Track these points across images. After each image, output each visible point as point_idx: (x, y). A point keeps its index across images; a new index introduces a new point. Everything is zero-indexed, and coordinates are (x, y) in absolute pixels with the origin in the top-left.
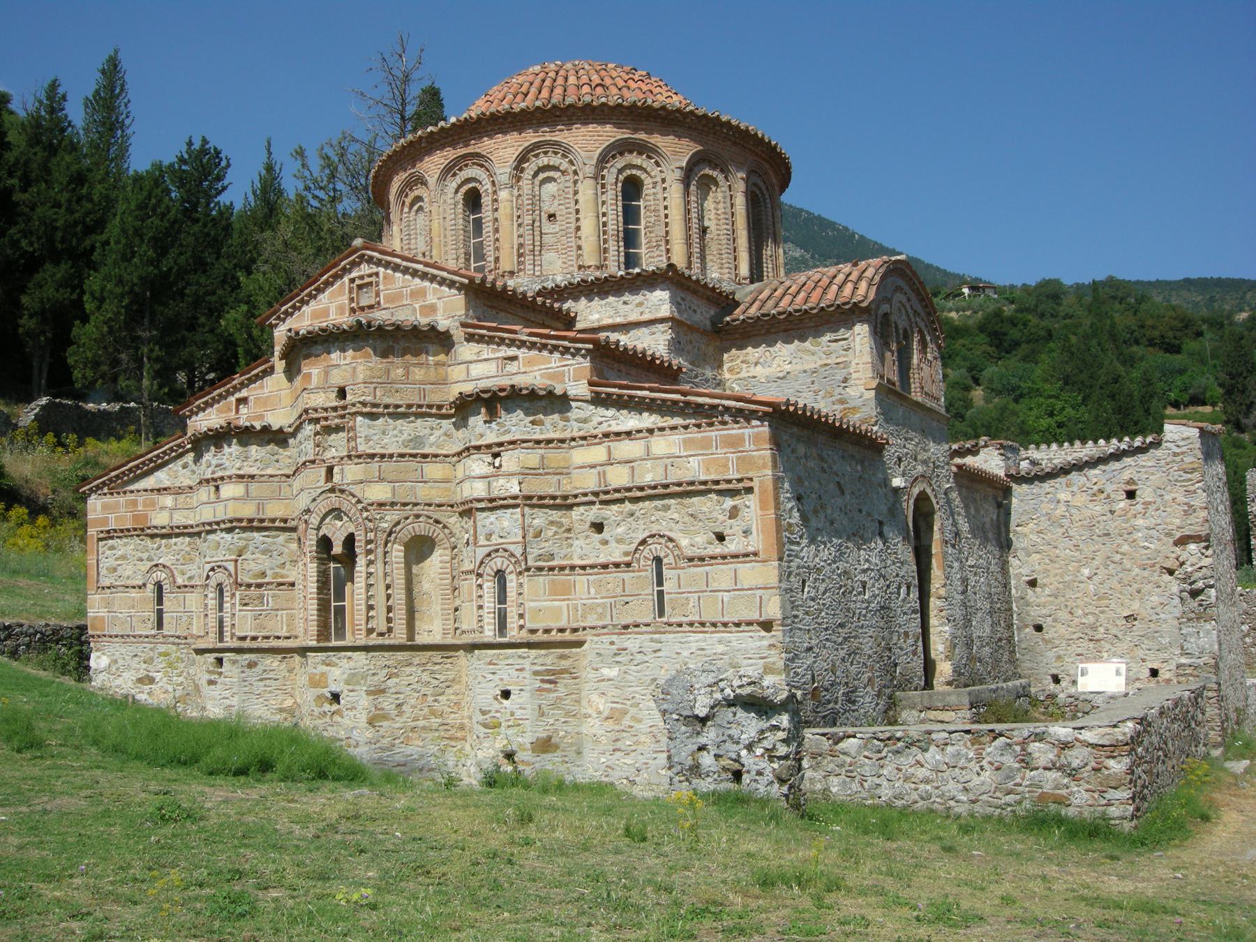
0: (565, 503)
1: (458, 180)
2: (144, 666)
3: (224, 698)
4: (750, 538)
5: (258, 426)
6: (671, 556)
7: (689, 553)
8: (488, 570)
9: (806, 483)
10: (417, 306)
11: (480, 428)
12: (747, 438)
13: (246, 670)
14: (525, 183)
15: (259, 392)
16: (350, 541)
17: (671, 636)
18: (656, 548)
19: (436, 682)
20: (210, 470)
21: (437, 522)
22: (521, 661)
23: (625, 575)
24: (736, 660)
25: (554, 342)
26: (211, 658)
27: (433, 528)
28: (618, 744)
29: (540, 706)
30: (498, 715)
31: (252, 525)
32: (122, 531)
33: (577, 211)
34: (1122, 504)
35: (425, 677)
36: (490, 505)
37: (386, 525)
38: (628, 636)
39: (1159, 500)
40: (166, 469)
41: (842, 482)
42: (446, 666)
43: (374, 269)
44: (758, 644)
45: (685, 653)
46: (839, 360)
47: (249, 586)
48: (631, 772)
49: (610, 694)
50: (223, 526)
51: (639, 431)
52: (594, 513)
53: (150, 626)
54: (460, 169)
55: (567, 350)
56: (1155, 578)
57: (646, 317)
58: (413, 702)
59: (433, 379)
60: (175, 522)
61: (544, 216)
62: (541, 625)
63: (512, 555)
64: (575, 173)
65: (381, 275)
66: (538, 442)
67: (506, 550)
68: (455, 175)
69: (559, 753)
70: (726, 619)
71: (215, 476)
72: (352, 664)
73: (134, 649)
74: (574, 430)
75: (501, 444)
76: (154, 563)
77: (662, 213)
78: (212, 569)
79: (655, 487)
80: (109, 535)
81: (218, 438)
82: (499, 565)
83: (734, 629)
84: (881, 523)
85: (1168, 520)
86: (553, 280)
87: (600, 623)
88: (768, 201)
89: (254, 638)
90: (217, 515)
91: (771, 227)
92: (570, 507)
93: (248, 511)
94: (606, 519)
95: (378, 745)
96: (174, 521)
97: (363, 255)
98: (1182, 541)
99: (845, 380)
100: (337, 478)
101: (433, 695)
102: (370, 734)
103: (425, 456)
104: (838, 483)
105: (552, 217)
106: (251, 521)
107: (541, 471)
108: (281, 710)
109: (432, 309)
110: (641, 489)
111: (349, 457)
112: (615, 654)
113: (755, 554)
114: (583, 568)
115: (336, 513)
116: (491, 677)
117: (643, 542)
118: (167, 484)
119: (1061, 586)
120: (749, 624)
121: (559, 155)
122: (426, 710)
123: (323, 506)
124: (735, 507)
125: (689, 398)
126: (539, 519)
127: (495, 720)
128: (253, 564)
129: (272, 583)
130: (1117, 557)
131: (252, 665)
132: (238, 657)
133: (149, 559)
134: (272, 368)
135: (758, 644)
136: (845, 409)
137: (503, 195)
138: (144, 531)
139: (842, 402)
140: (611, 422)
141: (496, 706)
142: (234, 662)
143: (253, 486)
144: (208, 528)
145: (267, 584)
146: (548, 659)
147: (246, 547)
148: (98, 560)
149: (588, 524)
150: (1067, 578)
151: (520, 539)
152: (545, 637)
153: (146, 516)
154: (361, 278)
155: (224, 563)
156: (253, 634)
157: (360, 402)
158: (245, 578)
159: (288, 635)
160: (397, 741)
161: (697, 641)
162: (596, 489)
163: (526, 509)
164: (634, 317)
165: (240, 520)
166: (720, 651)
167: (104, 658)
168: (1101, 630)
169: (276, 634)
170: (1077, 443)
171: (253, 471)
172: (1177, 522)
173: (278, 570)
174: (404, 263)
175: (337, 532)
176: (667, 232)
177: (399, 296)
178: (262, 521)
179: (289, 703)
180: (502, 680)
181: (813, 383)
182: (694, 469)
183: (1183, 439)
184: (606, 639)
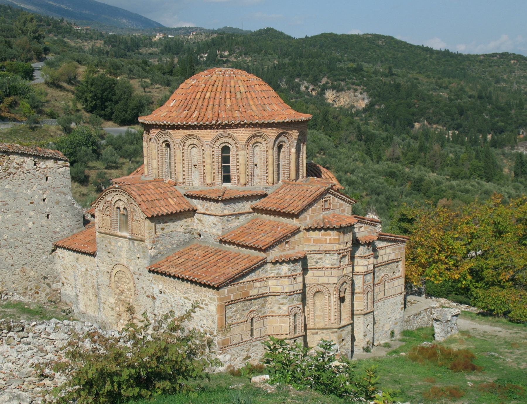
20: (290, 272)
32: (235, 300)
60: (260, 292)
71: (293, 274)
73: (242, 347)
153: (248, 292)
167: (228, 355)
182: (392, 257)
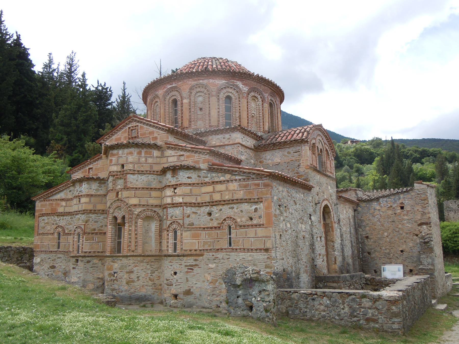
0: (199, 205)
1: (170, 96)
2: (52, 262)
3: (78, 274)
4: (261, 219)
5: (95, 177)
6: (234, 225)
7: (240, 224)
8: (171, 229)
9: (282, 200)
10: (151, 137)
11: (169, 178)
12: (261, 184)
13: (86, 263)
14: (192, 98)
15: (96, 166)
16: (124, 218)
17: (233, 253)
18: (229, 222)
19: (152, 269)
20: (78, 192)
21: (155, 211)
22: (181, 261)
23: (218, 231)
24: (256, 263)
25: (196, 150)
26: (74, 260)
27: (153, 213)
28: (214, 293)
29: (187, 278)
30: (172, 281)
31: (91, 212)
32: (47, 214)
33: (209, 107)
34: (399, 211)
35: (148, 267)
36: (173, 206)
37: (136, 213)
38: (219, 253)
39: (412, 210)
40: (63, 192)
41: (296, 200)
42: (156, 263)
43: (138, 124)
44: (263, 257)
45: (238, 260)
46: (296, 159)
47: (89, 233)
48: (218, 303)
49: (212, 274)
50: (81, 212)
51: (224, 181)
52: (207, 209)
53: (55, 248)
54: (171, 92)
55: (201, 152)
56: (411, 237)
57: (231, 143)
58: (143, 276)
59: (155, 162)
61: (198, 109)
62: (188, 248)
63: (179, 223)
64: (209, 94)
65: (139, 126)
66: (190, 184)
67: (177, 222)
68: (169, 94)
69: (193, 295)
70: (252, 248)
72: (122, 262)
74: (202, 180)
75: (177, 185)
76: (58, 225)
77: (238, 108)
78: (77, 228)
79: (229, 201)
80: (43, 215)
81: (80, 181)
82: (175, 227)
83: (255, 251)
84: (310, 215)
85: (416, 217)
86: (201, 131)
87: (209, 248)
88: (276, 106)
89: (90, 252)
90: (79, 208)
91: (276, 114)
92: (201, 206)
93: (90, 207)
94: (212, 211)
95: (129, 292)
96: (65, 210)
97: (133, 119)
98: (421, 224)
99: (299, 166)
100: (120, 196)
101: (150, 273)
102: (126, 287)
103: (151, 189)
104: (294, 201)
105: (201, 109)
106: (91, 210)
107: (190, 194)
108: (99, 278)
109: (156, 138)
110: (225, 201)
111: (124, 188)
112: (214, 259)
113: (263, 225)
114: (204, 228)
115: (119, 207)
116: (170, 267)
117: (225, 220)
118: (63, 197)
119: (377, 239)
120: (261, 249)
121: (204, 88)
122: (148, 279)
123: (115, 205)
124: (256, 209)
125: (241, 170)
126: (188, 210)
127: (171, 283)
128: (91, 226)
129: (98, 233)
130: (397, 229)
131: (89, 262)
132: (84, 259)
133: (56, 224)
134: (101, 157)
135: (263, 257)
136: (298, 175)
137: (185, 101)
138: (54, 213)
139: (297, 173)
140: (215, 178)
141: (172, 278)
142: (82, 261)
143: (92, 199)
144: (76, 213)
145: (96, 233)
146: (190, 261)
147: (89, 220)
148: (38, 224)
149: (206, 213)
150: (379, 236)
151: (182, 218)
152: (190, 253)
153: (56, 209)
154: (133, 127)
155: (81, 226)
156: (90, 251)
157: (129, 170)
158: (88, 231)
159: (102, 251)
160: (137, 290)
161: (242, 255)
162: (209, 201)
163: (185, 207)
164: (226, 143)
165: (87, 210)
166: (250, 259)
168: (392, 255)
169: (98, 251)
170: (383, 190)
171: (93, 193)
172: (419, 218)
173: (100, 228)
174: (147, 122)
175: (119, 216)
176: (240, 116)
177: (145, 134)
178: (95, 210)
179: (101, 276)
180: (174, 268)
181: (288, 166)
183: (421, 189)
184: (211, 254)
